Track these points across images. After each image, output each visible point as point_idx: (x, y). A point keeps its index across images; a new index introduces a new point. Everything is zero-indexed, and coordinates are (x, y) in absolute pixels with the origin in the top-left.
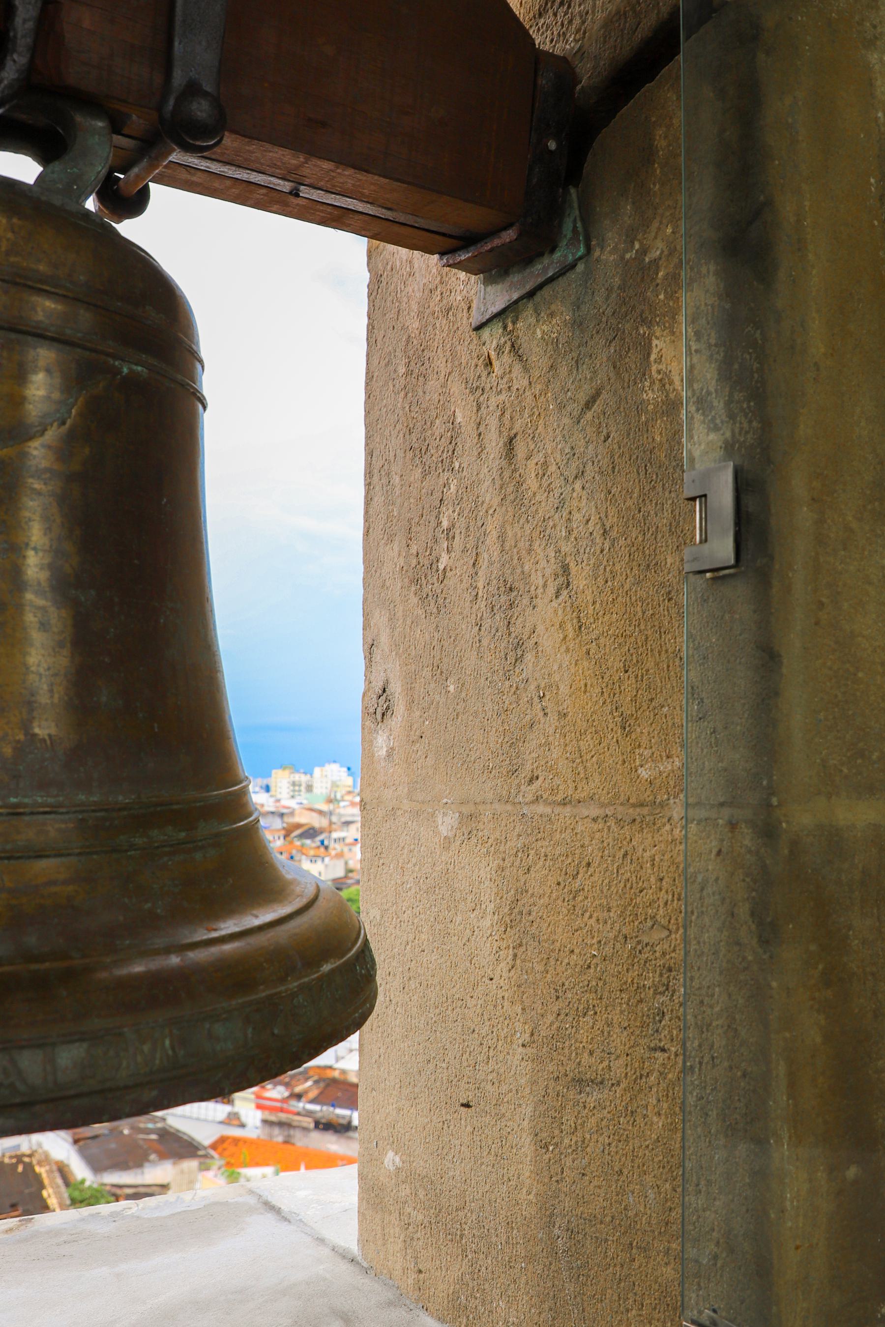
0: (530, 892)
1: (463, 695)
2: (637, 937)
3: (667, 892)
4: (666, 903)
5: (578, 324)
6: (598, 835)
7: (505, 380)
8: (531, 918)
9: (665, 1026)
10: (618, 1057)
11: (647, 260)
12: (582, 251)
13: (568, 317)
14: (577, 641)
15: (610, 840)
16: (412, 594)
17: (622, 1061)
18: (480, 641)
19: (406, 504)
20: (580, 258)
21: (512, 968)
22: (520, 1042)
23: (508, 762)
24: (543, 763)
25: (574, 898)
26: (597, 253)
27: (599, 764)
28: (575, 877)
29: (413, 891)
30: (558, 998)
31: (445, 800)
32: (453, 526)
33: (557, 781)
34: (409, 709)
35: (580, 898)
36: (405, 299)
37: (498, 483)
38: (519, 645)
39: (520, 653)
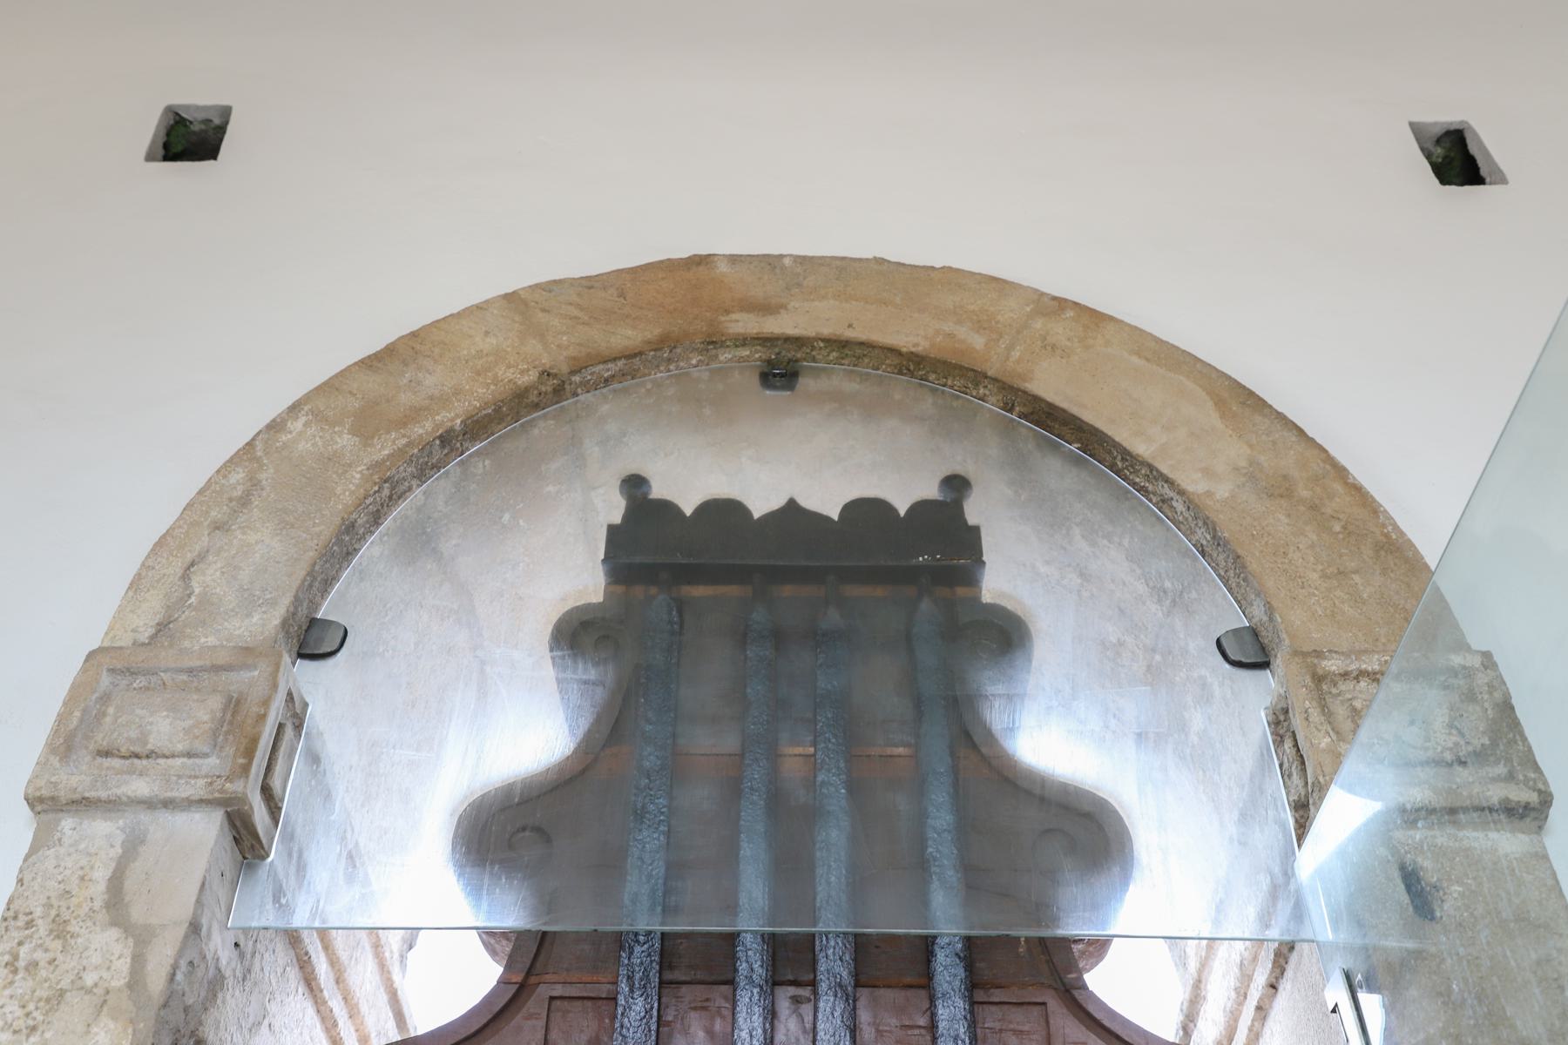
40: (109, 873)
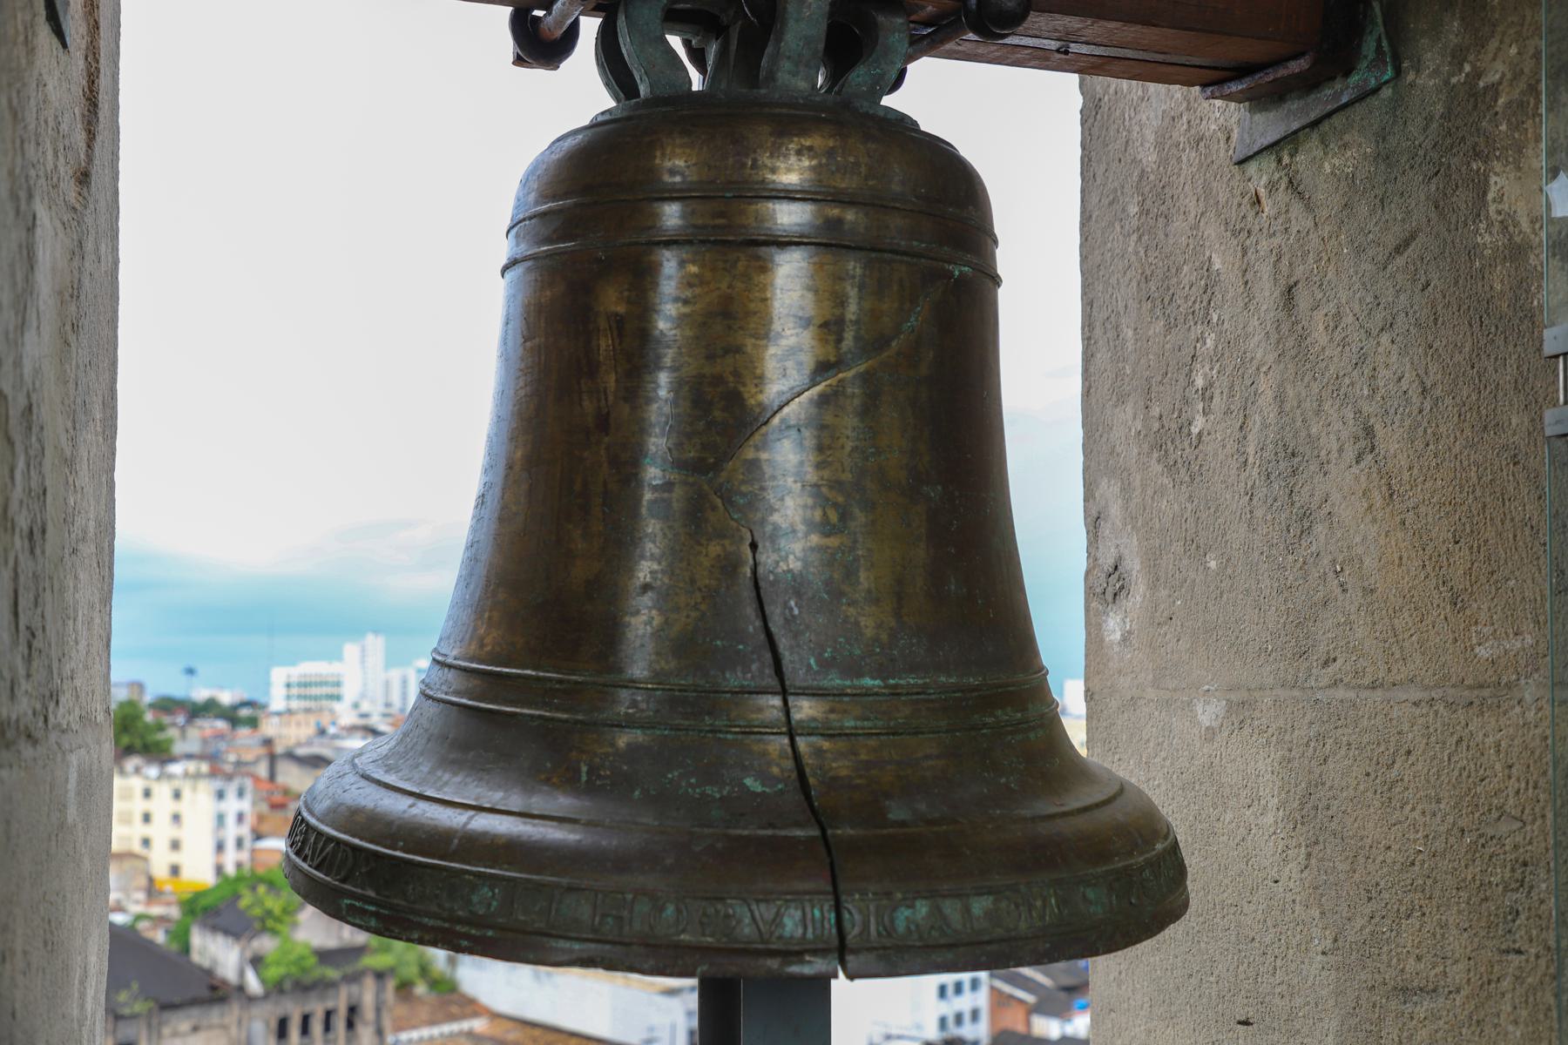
0: (1328, 784)
1: (1229, 571)
2: (1478, 830)
3: (1518, 780)
5: (1384, 158)
6: (1421, 721)
7: (1280, 221)
8: (1330, 813)
9: (1520, 926)
10: (1456, 962)
11: (1481, 84)
12: (1389, 73)
13: (1368, 150)
14: (1388, 510)
16: (1154, 461)
17: (1461, 966)
18: (1251, 512)
19: (1142, 361)
20: (1387, 82)
21: (1306, 868)
23: (1293, 643)
25: (1390, 789)
26: (1411, 77)
27: (1421, 643)
28: (1390, 766)
29: (1164, 788)
30: (1370, 899)
31: (1206, 687)
32: (1211, 385)
33: (1362, 663)
34: (1153, 586)
35: (1398, 790)
36: (1137, 128)
37: (1274, 337)
38: (1306, 515)
39: (1306, 525)
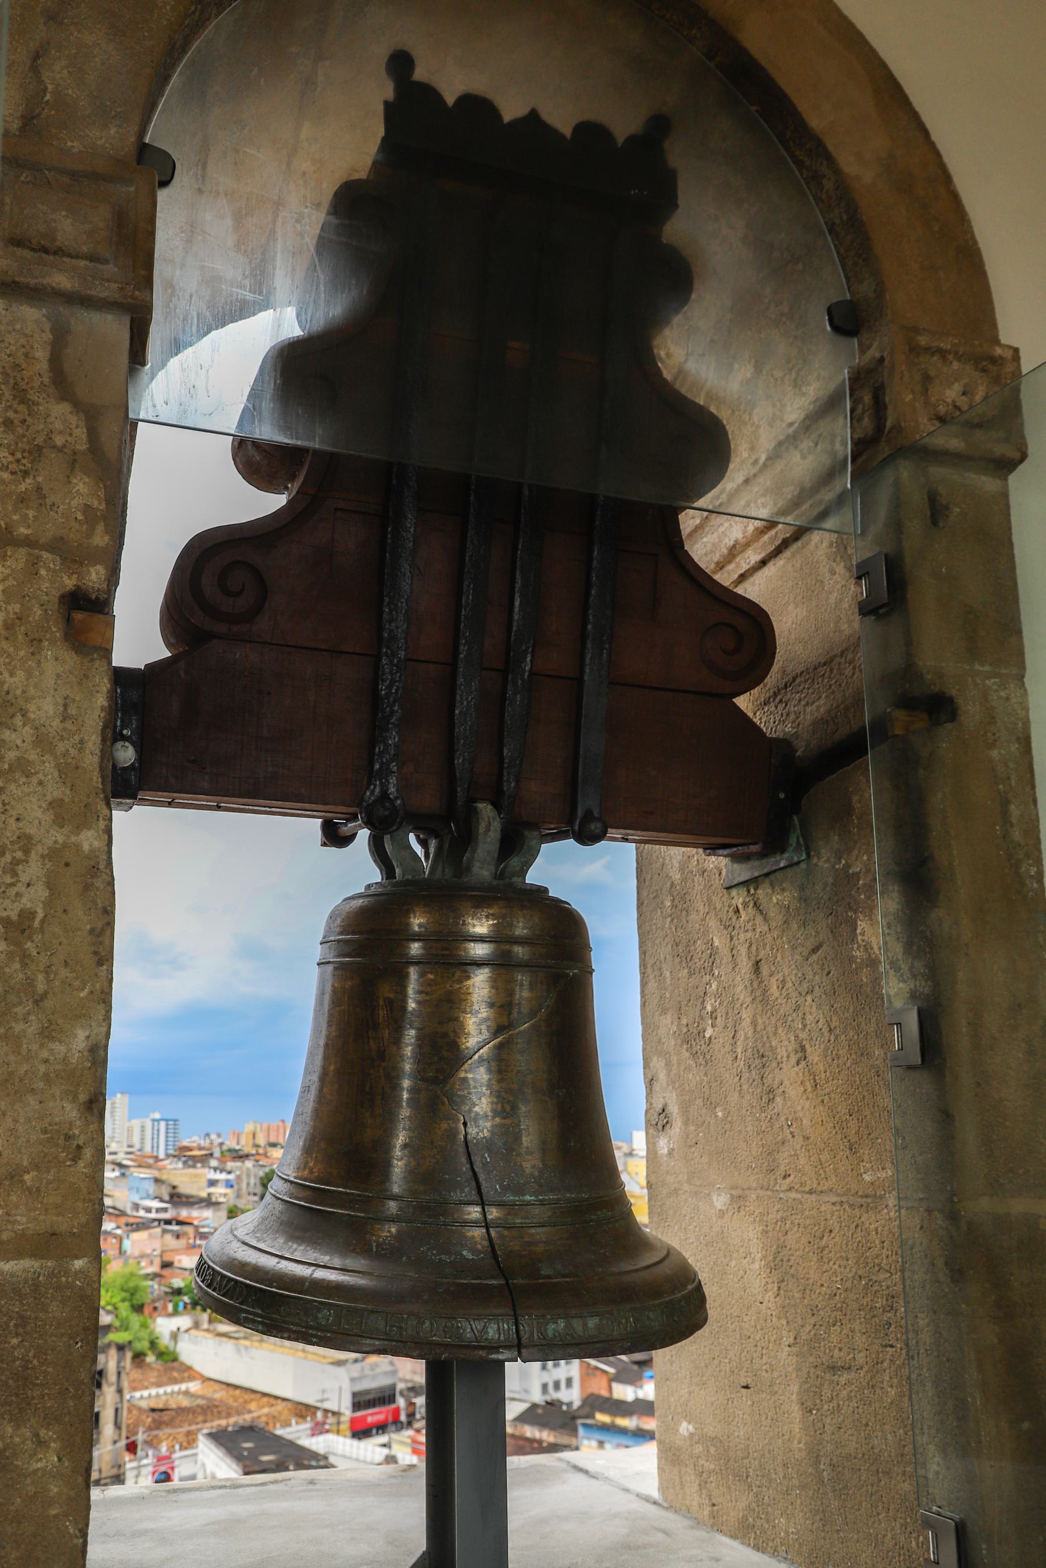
0: (789, 1247)
1: (729, 1119)
4: (887, 1257)
6: (836, 1213)
8: (790, 1264)
15: (846, 1217)
22: (787, 1343)
23: (766, 1164)
24: (793, 1166)
28: (821, 1238)
30: (813, 1315)
31: (718, 1186)
33: (804, 1178)
37: (749, 989)
39: (771, 1097)
40: (48, 355)
